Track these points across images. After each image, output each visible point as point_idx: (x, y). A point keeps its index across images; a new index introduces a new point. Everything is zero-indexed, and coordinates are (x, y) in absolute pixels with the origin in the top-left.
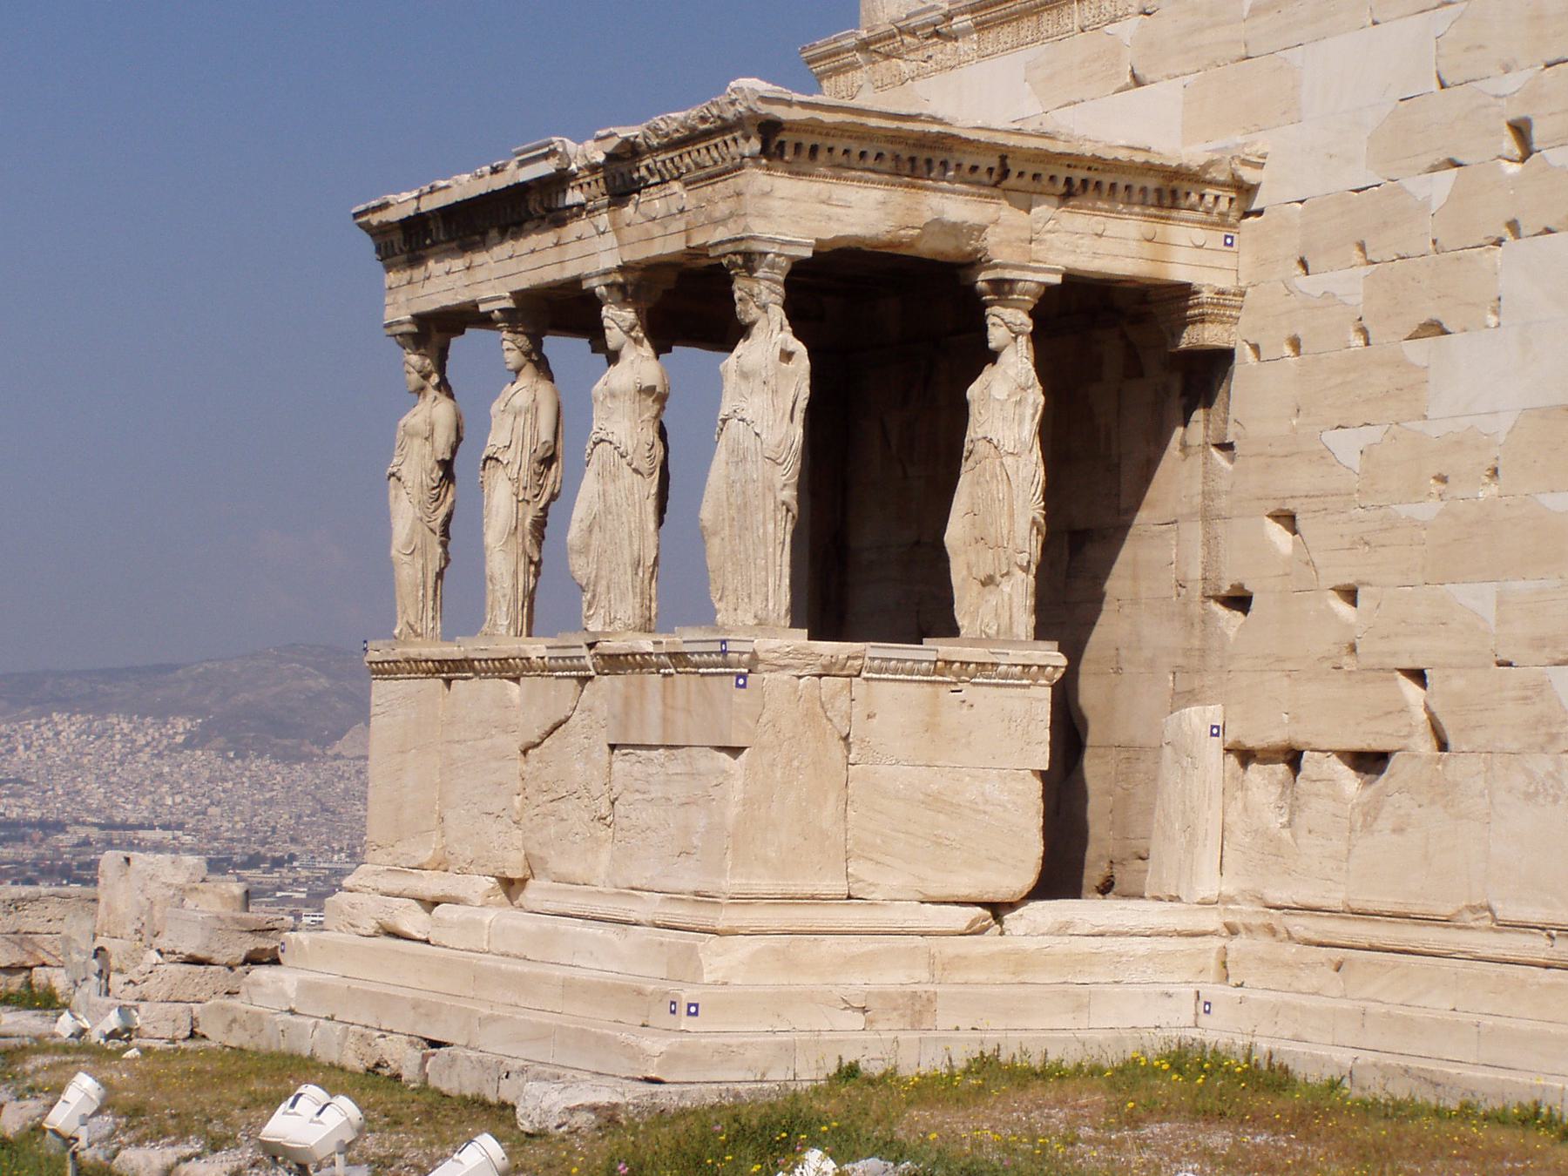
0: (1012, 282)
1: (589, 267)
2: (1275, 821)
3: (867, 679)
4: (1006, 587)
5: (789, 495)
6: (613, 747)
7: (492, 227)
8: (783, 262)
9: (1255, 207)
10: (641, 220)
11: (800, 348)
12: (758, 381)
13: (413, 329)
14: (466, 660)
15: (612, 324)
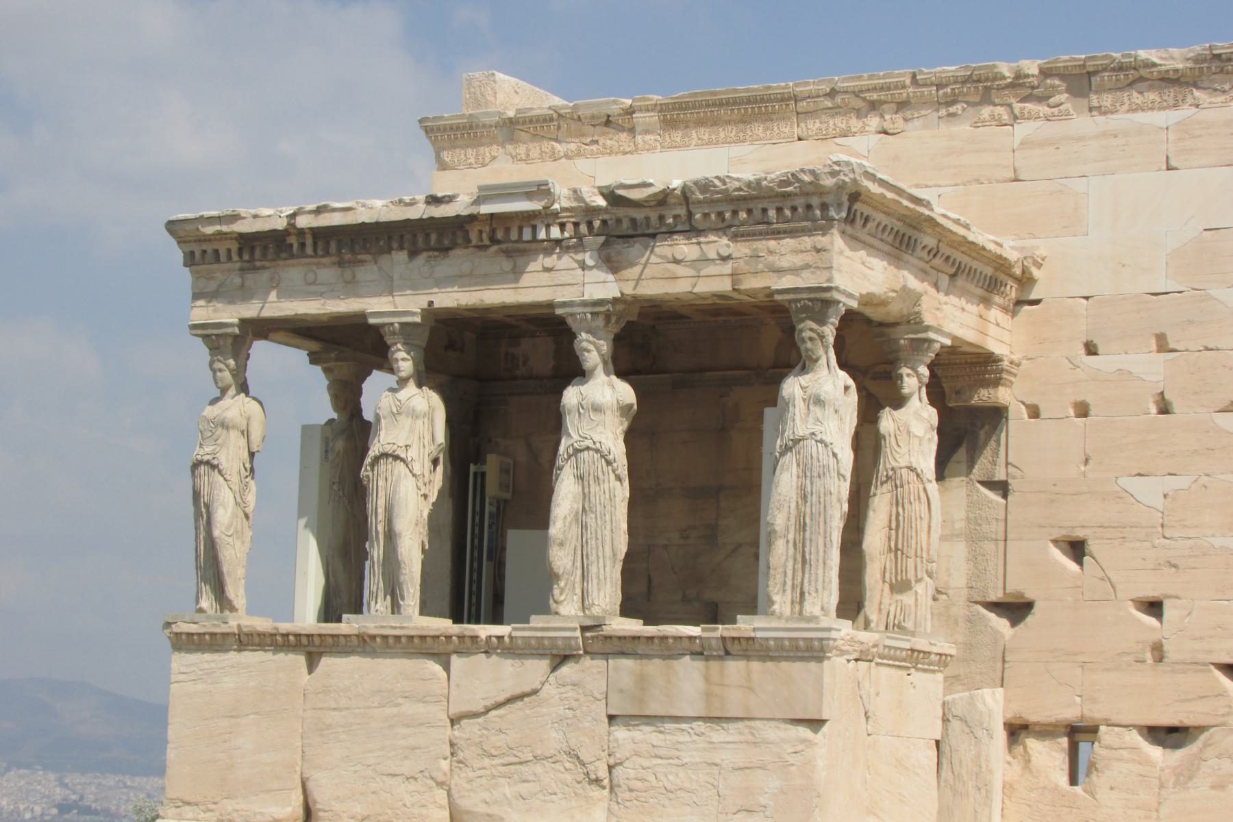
0: (930, 341)
1: (561, 296)
2: (1063, 780)
3: (877, 664)
4: (919, 588)
5: (846, 507)
6: (611, 718)
7: (401, 248)
8: (843, 310)
9: (1033, 297)
10: (659, 260)
11: (851, 382)
12: (832, 409)
13: (237, 331)
14: (357, 636)
15: (591, 347)
